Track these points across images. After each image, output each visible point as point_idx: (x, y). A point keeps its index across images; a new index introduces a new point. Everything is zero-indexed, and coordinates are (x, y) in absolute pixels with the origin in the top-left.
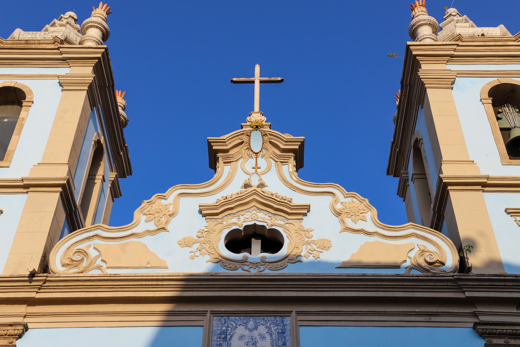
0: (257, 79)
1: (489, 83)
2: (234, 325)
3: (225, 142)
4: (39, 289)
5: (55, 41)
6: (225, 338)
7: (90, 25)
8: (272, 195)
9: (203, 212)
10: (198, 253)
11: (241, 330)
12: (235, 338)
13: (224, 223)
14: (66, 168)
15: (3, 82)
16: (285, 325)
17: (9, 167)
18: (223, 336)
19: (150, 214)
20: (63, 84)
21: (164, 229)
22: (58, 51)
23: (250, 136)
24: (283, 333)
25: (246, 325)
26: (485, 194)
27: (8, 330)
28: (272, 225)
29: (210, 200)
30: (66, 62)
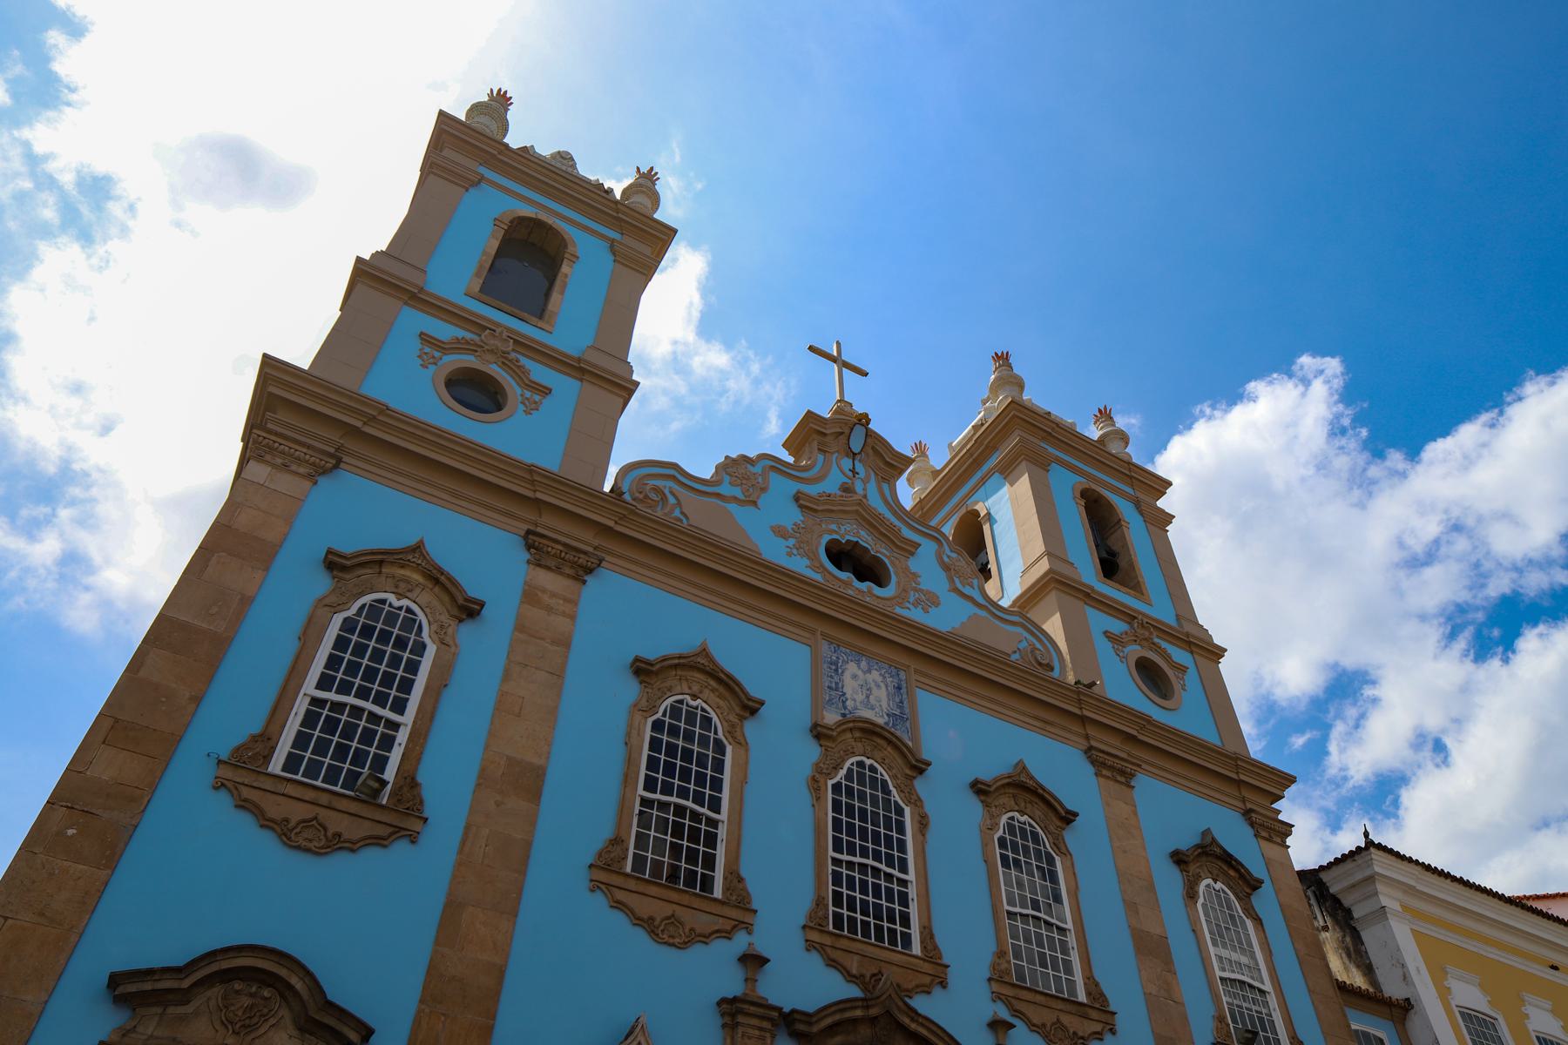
3: (826, 424)
4: (620, 519)
6: (836, 670)
8: (880, 514)
9: (801, 502)
10: (795, 552)
13: (824, 526)
16: (900, 680)
18: (834, 667)
19: (736, 477)
21: (754, 503)
23: (852, 429)
24: (899, 688)
25: (858, 662)
26: (1086, 607)
28: (877, 552)
29: (813, 490)
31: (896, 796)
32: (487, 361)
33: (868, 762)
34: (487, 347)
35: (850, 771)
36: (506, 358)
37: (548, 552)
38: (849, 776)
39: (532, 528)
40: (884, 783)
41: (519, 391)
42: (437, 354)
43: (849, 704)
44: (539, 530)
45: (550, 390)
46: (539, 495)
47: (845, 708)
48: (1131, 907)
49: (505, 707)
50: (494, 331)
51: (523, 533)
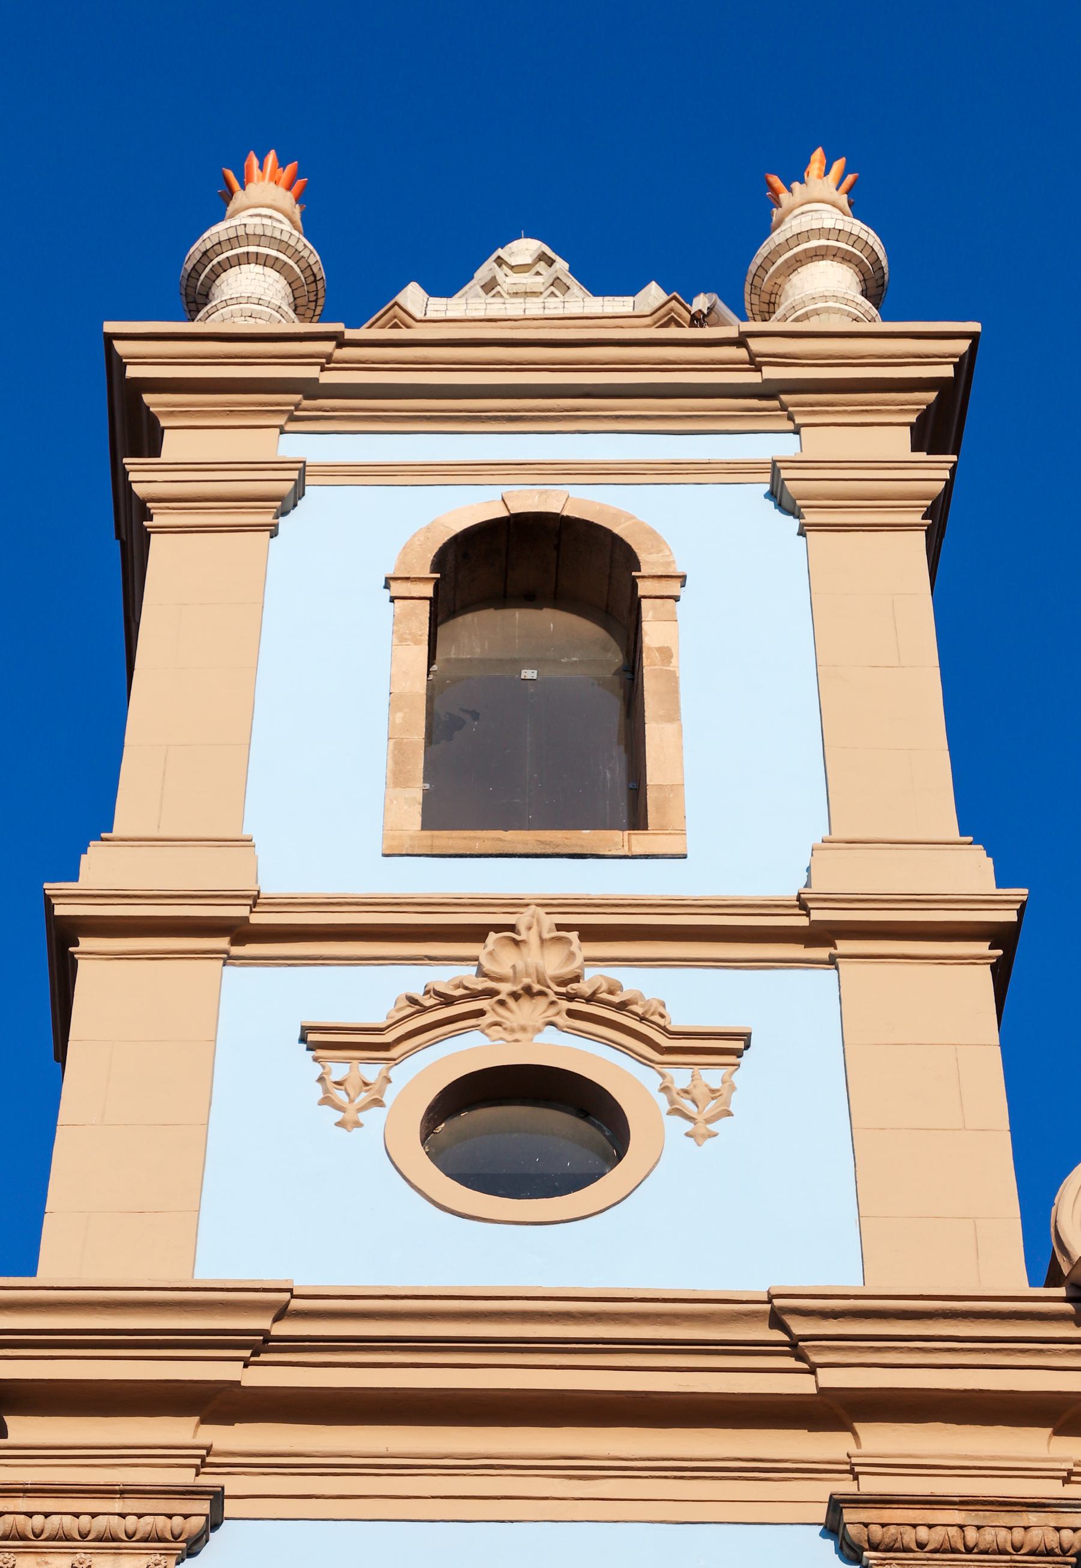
5: (666, 319)
7: (816, 248)
20: (800, 499)
22: (741, 353)
27: (1026, 1528)
30: (775, 403)
32: (524, 1029)
34: (505, 988)
36: (570, 997)
37: (921, 1546)
39: (846, 1486)
41: (649, 1078)
42: (371, 1072)
44: (870, 1485)
45: (745, 1037)
46: (830, 1378)
50: (512, 928)
51: (820, 1513)
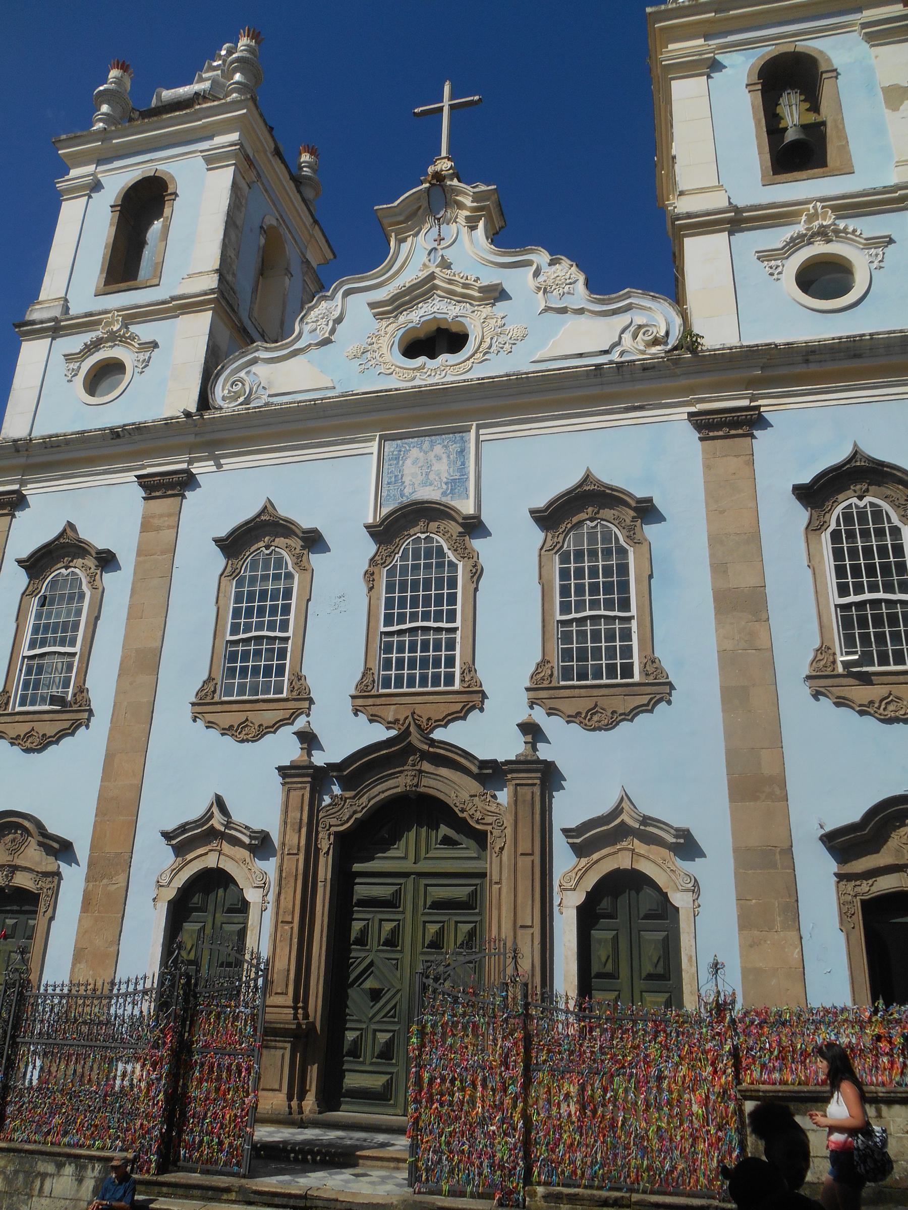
0: (446, 103)
1: (763, 56)
2: (408, 448)
11: (415, 452)
12: (408, 462)
14: (216, 277)
15: (142, 172)
17: (158, 285)
19: (313, 322)
29: (382, 294)
31: (451, 555)
33: (423, 536)
35: (406, 550)
38: (404, 557)
40: (440, 549)
43: (407, 491)
47: (402, 495)
48: (719, 568)
49: (134, 614)
